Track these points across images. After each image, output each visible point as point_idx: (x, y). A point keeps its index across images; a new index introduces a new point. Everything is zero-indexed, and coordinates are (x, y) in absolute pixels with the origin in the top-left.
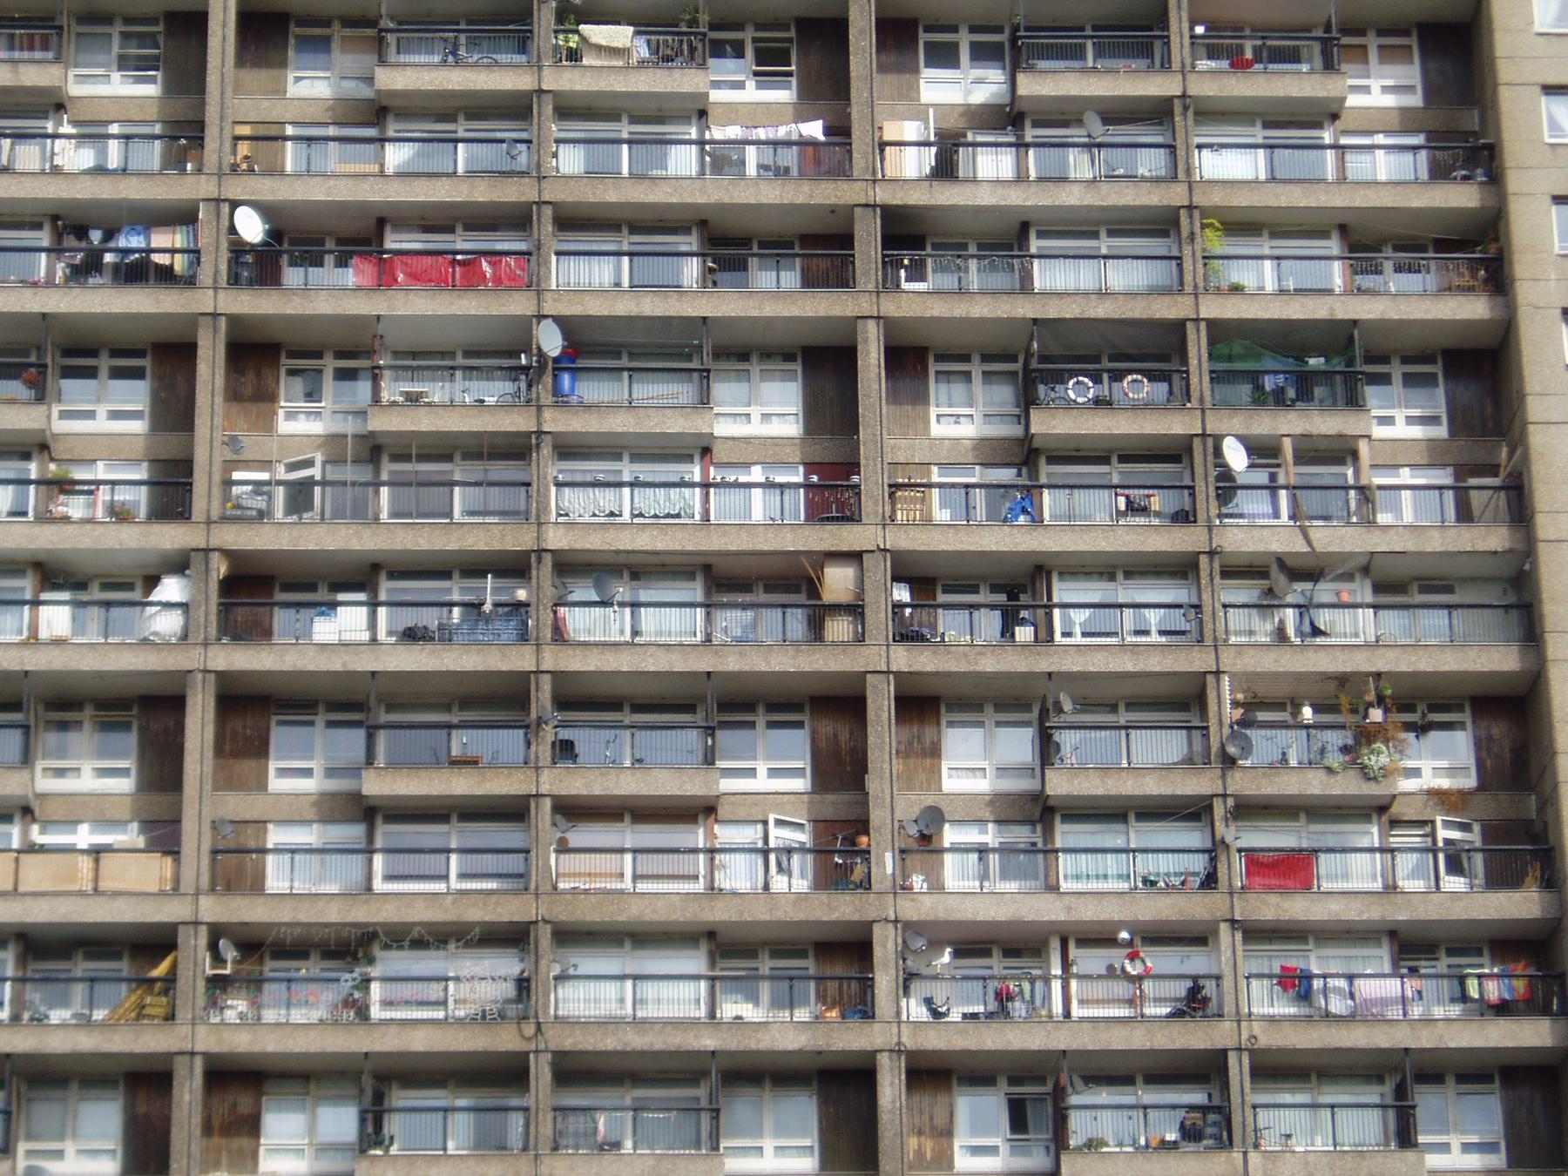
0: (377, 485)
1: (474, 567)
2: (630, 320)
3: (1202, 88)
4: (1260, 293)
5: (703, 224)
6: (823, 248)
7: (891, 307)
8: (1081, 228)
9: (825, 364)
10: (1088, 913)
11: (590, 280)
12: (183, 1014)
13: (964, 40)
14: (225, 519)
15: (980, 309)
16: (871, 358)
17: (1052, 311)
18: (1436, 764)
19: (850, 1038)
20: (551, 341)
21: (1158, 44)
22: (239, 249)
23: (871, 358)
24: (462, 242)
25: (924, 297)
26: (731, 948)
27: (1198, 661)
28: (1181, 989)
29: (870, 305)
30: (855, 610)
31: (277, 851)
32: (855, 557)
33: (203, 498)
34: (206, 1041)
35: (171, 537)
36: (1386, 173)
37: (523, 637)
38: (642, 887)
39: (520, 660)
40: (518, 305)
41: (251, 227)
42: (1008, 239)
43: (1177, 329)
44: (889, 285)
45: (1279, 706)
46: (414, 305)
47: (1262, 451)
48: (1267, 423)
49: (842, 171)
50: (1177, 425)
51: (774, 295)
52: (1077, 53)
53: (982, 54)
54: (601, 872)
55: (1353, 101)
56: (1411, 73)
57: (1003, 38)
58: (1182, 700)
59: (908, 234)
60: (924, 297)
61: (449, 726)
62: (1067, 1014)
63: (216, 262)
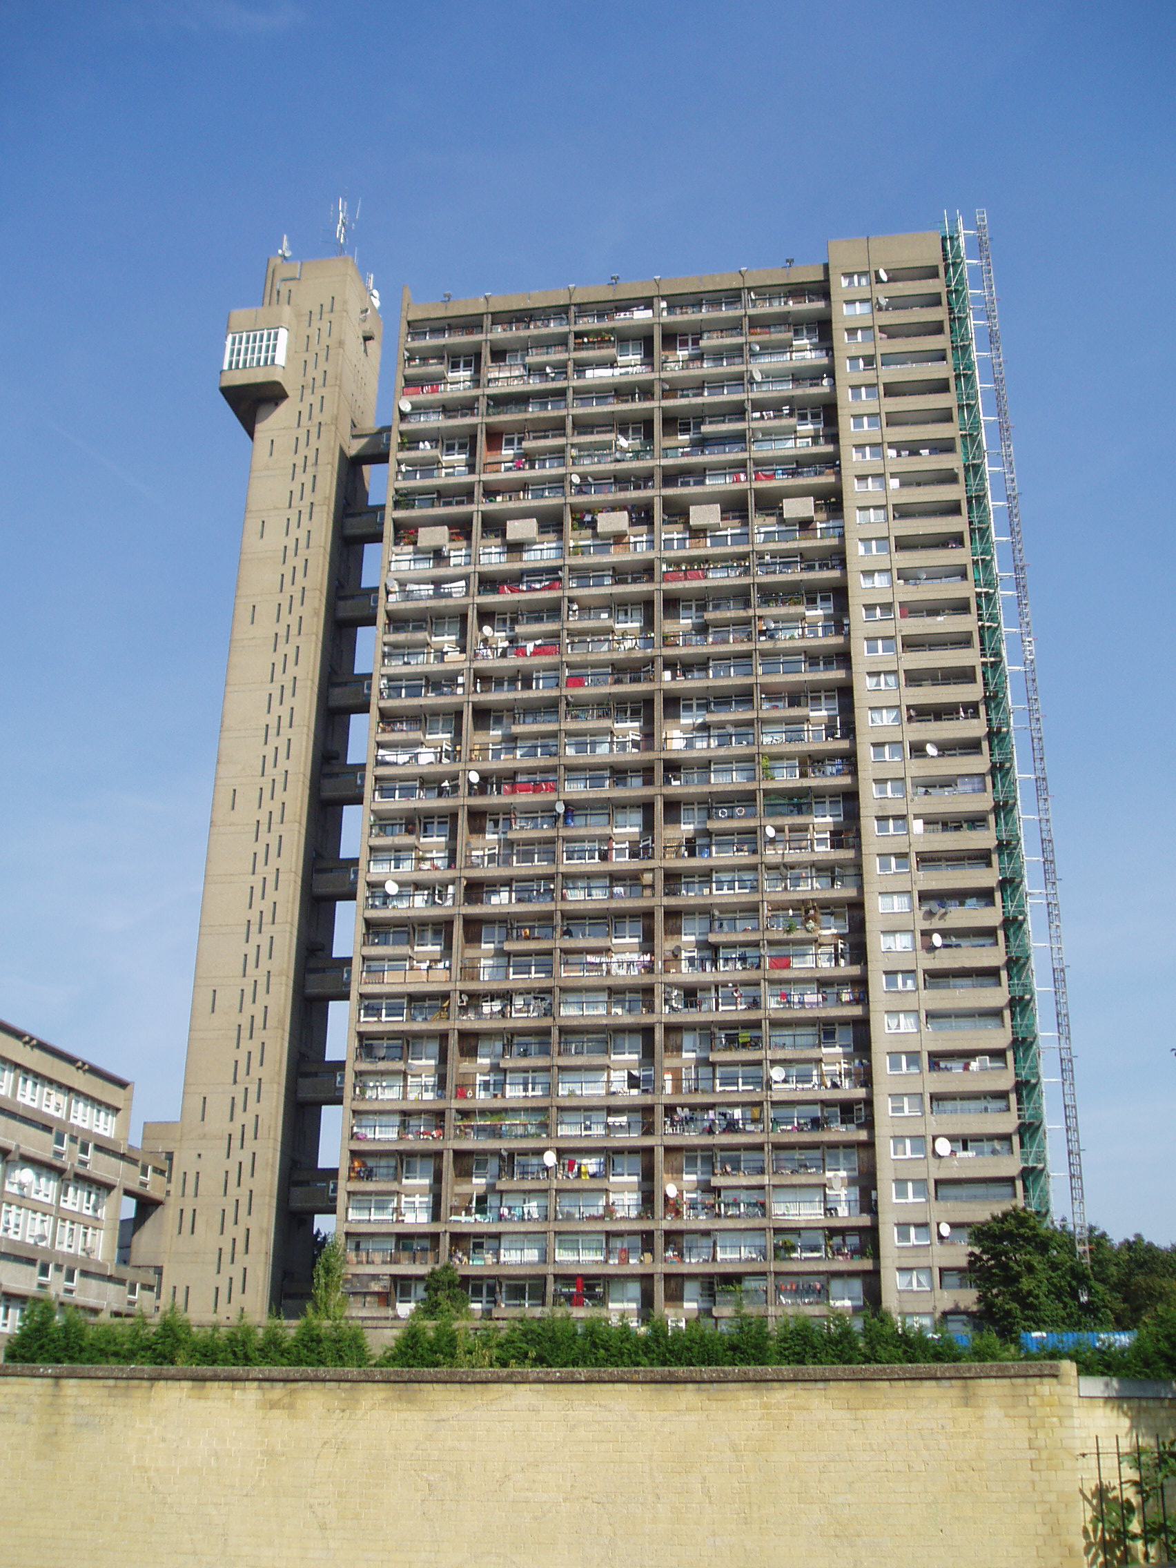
1: (539, 878)
3: (763, 715)
5: (611, 767)
6: (646, 772)
7: (667, 790)
8: (726, 763)
9: (647, 807)
11: (576, 789)
12: (452, 1017)
13: (694, 703)
14: (466, 867)
15: (692, 789)
19: (647, 1019)
20: (560, 808)
22: (471, 785)
24: (538, 777)
25: (676, 787)
27: (756, 897)
28: (751, 1000)
29: (658, 792)
30: (652, 886)
32: (652, 870)
33: (460, 861)
34: (458, 1025)
35: (451, 874)
36: (814, 740)
37: (553, 899)
39: (551, 907)
40: (552, 797)
41: (474, 777)
42: (705, 765)
43: (754, 792)
44: (667, 781)
46: (523, 798)
47: (779, 830)
48: (779, 821)
49: (650, 748)
50: (752, 823)
51: (635, 789)
54: (567, 974)
59: (673, 767)
60: (676, 787)
63: (463, 790)
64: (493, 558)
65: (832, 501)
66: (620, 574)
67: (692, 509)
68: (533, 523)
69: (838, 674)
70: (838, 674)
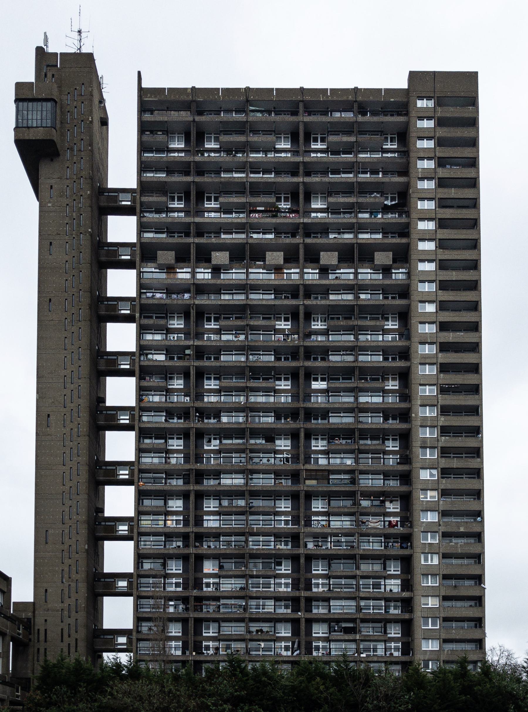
0: (220, 457)
2: (262, 428)
4: (367, 423)
10: (335, 531)
16: (302, 435)
17: (333, 427)
18: (393, 507)
21: (353, 377)
23: (302, 435)
26: (278, 536)
31: (205, 520)
38: (263, 547)
45: (368, 497)
52: (339, 379)
53: (323, 380)
55: (386, 388)
56: (397, 383)
57: (326, 376)
58: (351, 495)
61: (232, 499)
62: (331, 547)
64: (204, 275)
65: (403, 256)
66: (278, 290)
67: (322, 253)
68: (227, 254)
69: (400, 364)
70: (400, 364)
